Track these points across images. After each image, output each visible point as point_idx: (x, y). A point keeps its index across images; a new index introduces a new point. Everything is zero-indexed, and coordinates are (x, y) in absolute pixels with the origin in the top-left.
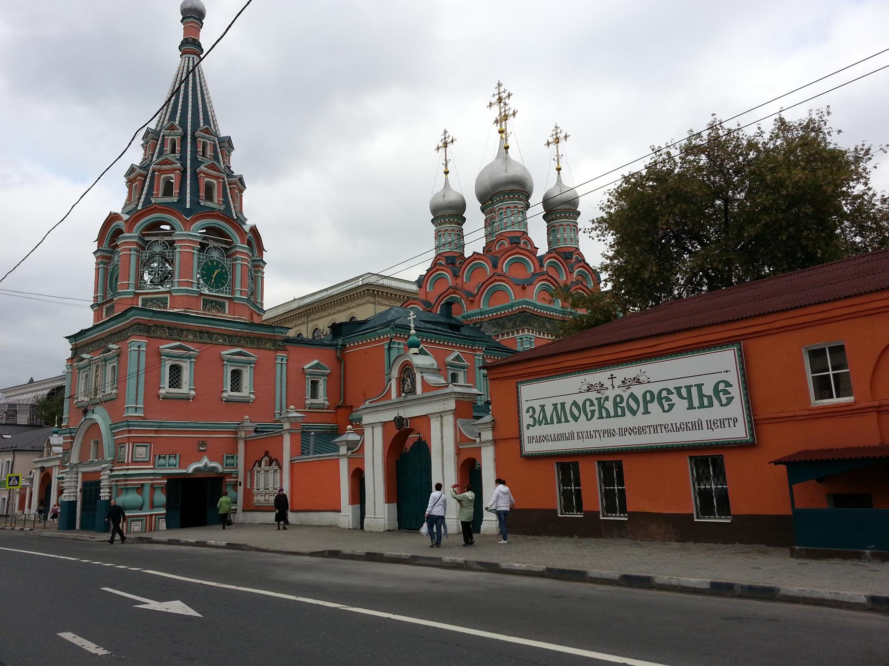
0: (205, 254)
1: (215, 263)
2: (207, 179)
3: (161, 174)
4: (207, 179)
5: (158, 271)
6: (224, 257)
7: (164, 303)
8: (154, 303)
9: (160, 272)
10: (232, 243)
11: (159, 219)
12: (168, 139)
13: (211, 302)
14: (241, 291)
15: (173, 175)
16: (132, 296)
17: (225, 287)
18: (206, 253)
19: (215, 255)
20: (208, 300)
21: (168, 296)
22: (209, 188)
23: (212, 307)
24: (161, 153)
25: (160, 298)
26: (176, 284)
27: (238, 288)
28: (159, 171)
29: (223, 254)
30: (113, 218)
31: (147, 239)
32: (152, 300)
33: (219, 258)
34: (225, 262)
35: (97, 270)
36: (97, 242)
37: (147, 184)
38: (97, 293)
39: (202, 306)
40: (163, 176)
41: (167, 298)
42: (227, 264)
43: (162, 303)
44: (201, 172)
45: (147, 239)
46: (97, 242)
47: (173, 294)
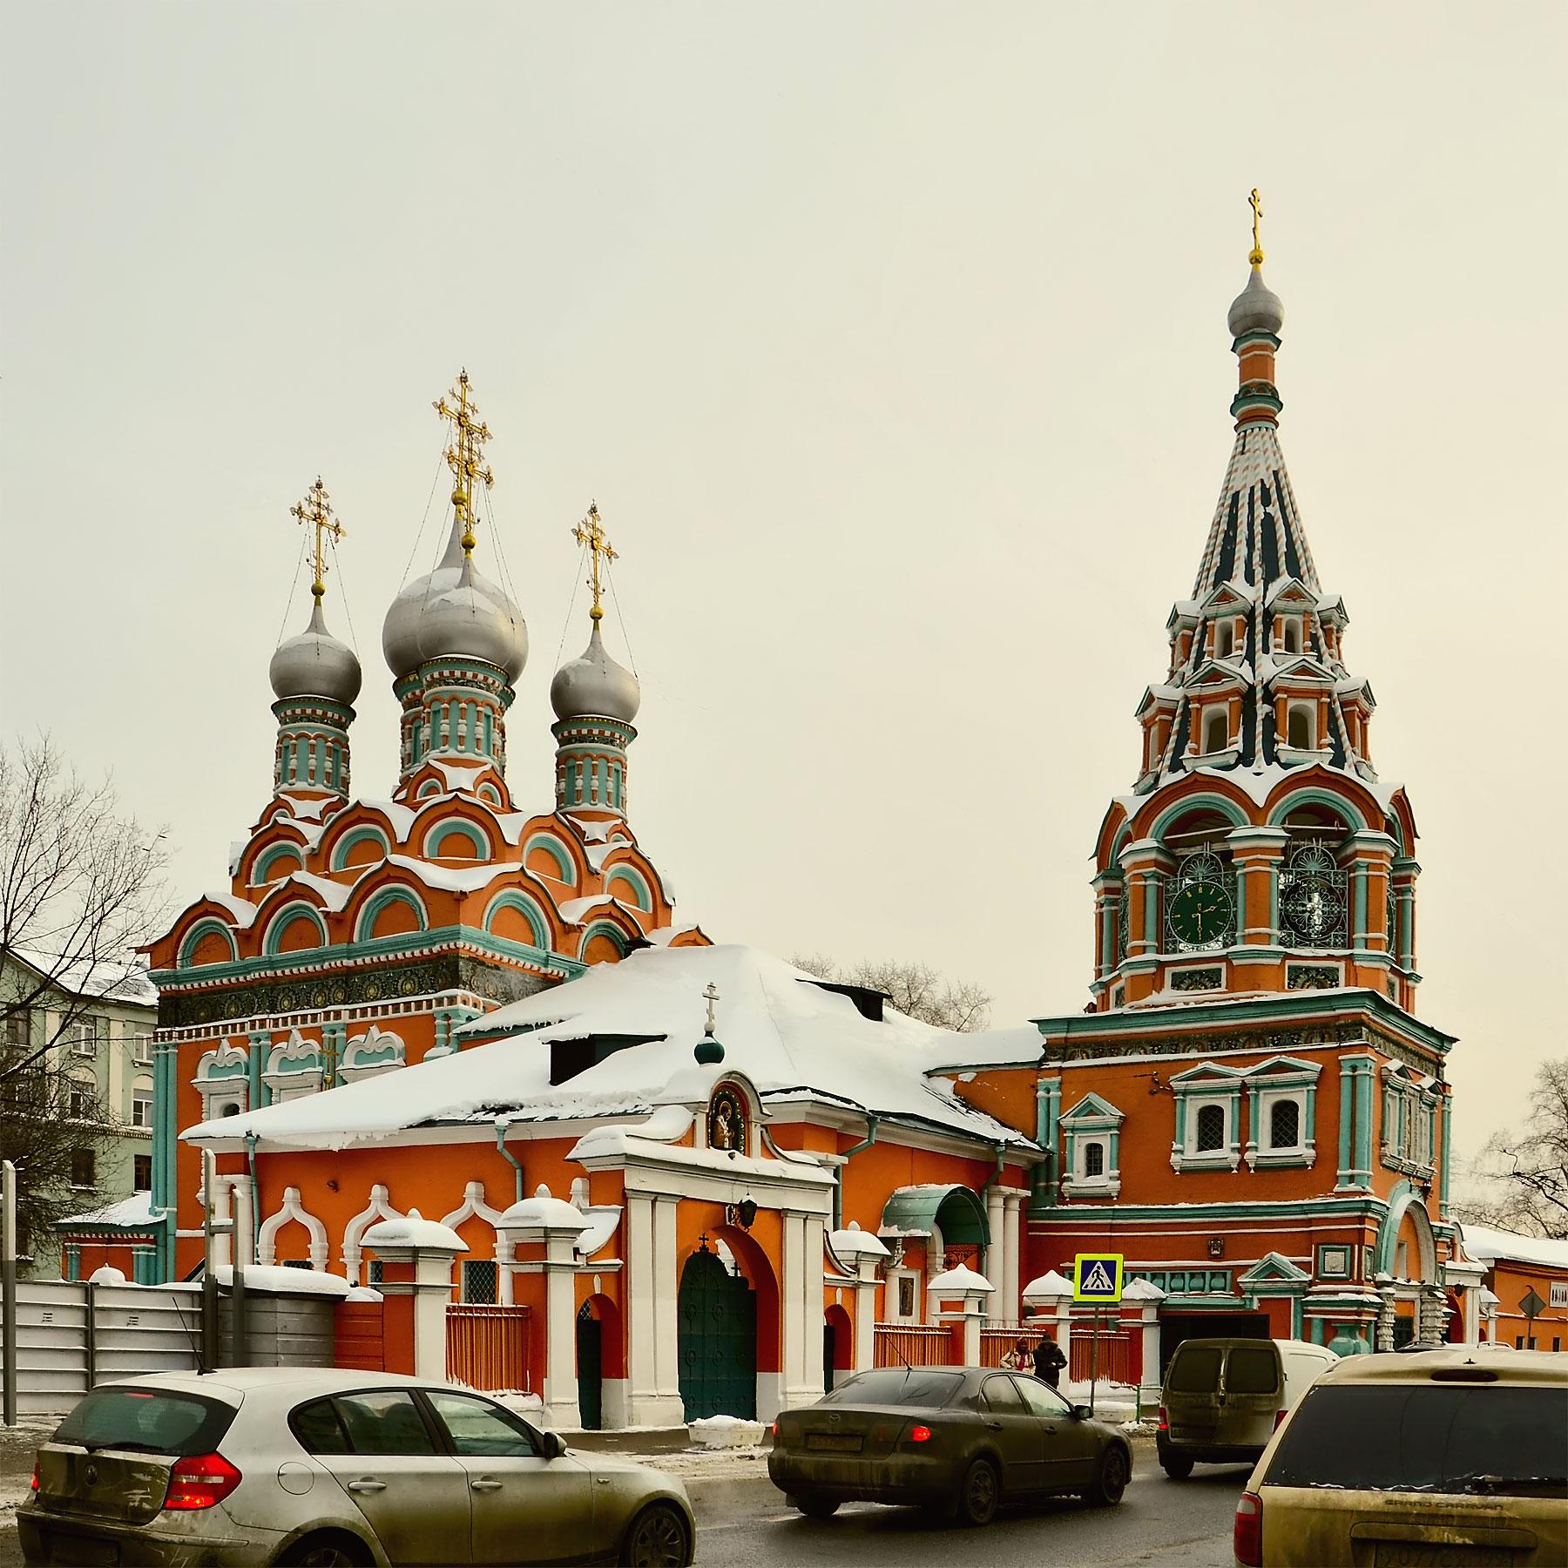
2: (1292, 703)
3: (1202, 705)
4: (1292, 703)
7: (1215, 979)
8: (1196, 981)
10: (1346, 837)
11: (1198, 806)
12: (1213, 626)
13: (1308, 969)
14: (1366, 940)
15: (1224, 707)
16: (1153, 970)
20: (1300, 968)
21: (1223, 966)
22: (1299, 720)
23: (1308, 981)
24: (1200, 654)
25: (1206, 971)
26: (1239, 940)
27: (1360, 935)
28: (1201, 700)
30: (1116, 811)
31: (1180, 852)
32: (1192, 973)
35: (1100, 916)
36: (1096, 858)
37: (1176, 727)
38: (1101, 964)
39: (1286, 981)
40: (1207, 709)
42: (1336, 882)
43: (1210, 980)
44: (1278, 690)
45: (1180, 852)
46: (1096, 858)
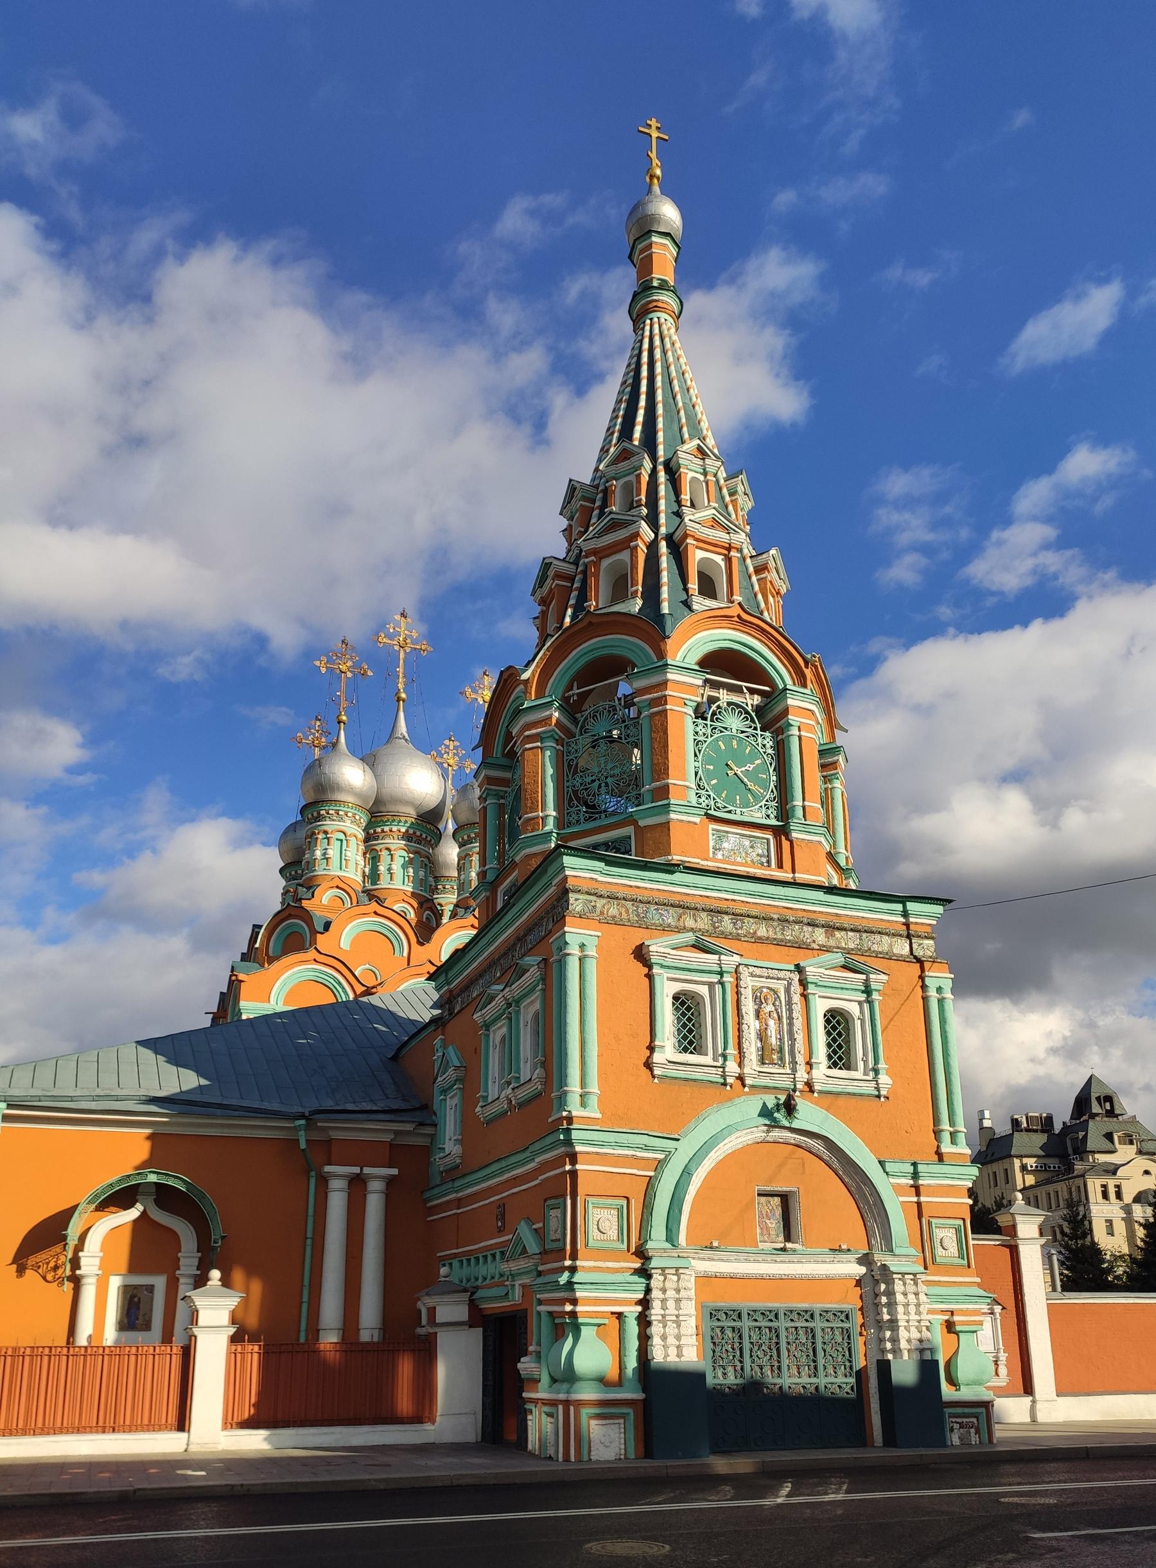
0: (709, 722)
1: (735, 742)
5: (606, 778)
6: (755, 729)
9: (609, 780)
17: (764, 802)
18: (712, 721)
19: (734, 722)
21: (629, 830)
26: (647, 797)
29: (753, 721)
33: (743, 732)
34: (760, 740)
41: (630, 838)
42: (764, 746)
47: (642, 823)
